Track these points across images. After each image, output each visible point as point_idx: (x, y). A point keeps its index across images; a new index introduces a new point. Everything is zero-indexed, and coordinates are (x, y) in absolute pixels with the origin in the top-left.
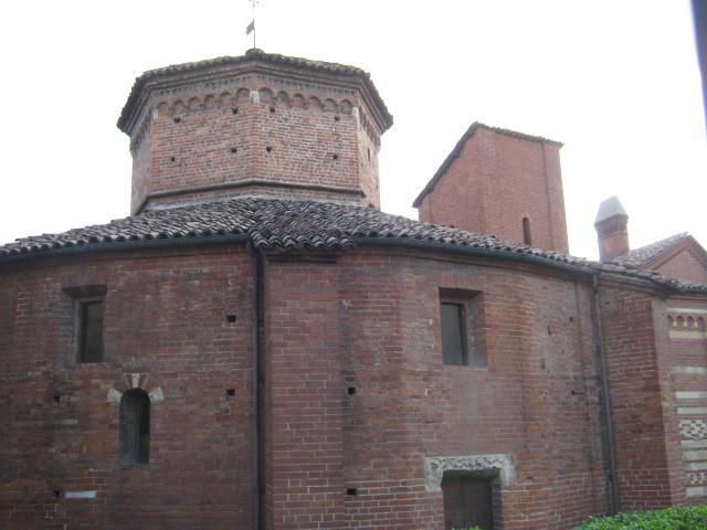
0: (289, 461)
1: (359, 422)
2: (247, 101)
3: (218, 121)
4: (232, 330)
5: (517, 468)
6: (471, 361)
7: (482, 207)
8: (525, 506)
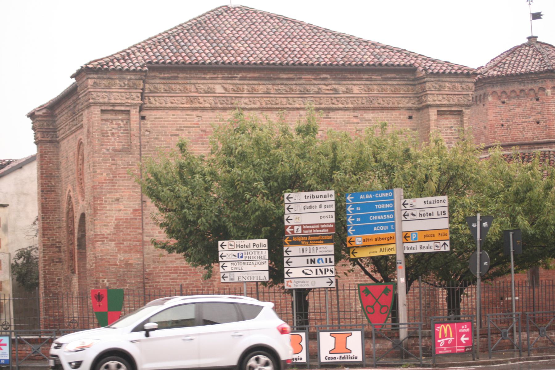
2: (544, 94)
3: (527, 104)
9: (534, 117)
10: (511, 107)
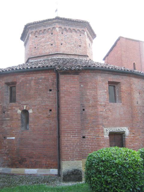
0: (66, 129)
1: (86, 118)
4: (50, 93)
5: (130, 131)
6: (117, 102)
7: (122, 60)
8: (132, 141)
9: (50, 42)
10: (40, 39)
